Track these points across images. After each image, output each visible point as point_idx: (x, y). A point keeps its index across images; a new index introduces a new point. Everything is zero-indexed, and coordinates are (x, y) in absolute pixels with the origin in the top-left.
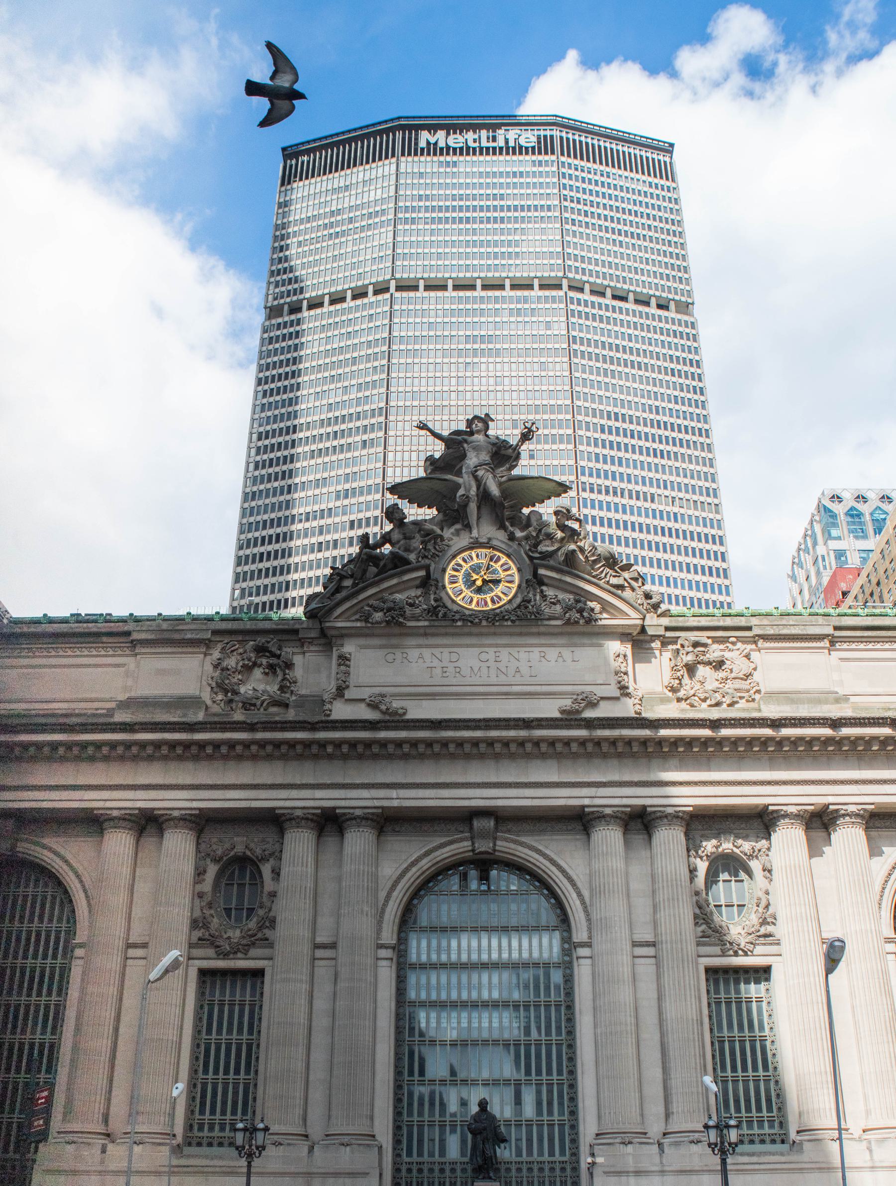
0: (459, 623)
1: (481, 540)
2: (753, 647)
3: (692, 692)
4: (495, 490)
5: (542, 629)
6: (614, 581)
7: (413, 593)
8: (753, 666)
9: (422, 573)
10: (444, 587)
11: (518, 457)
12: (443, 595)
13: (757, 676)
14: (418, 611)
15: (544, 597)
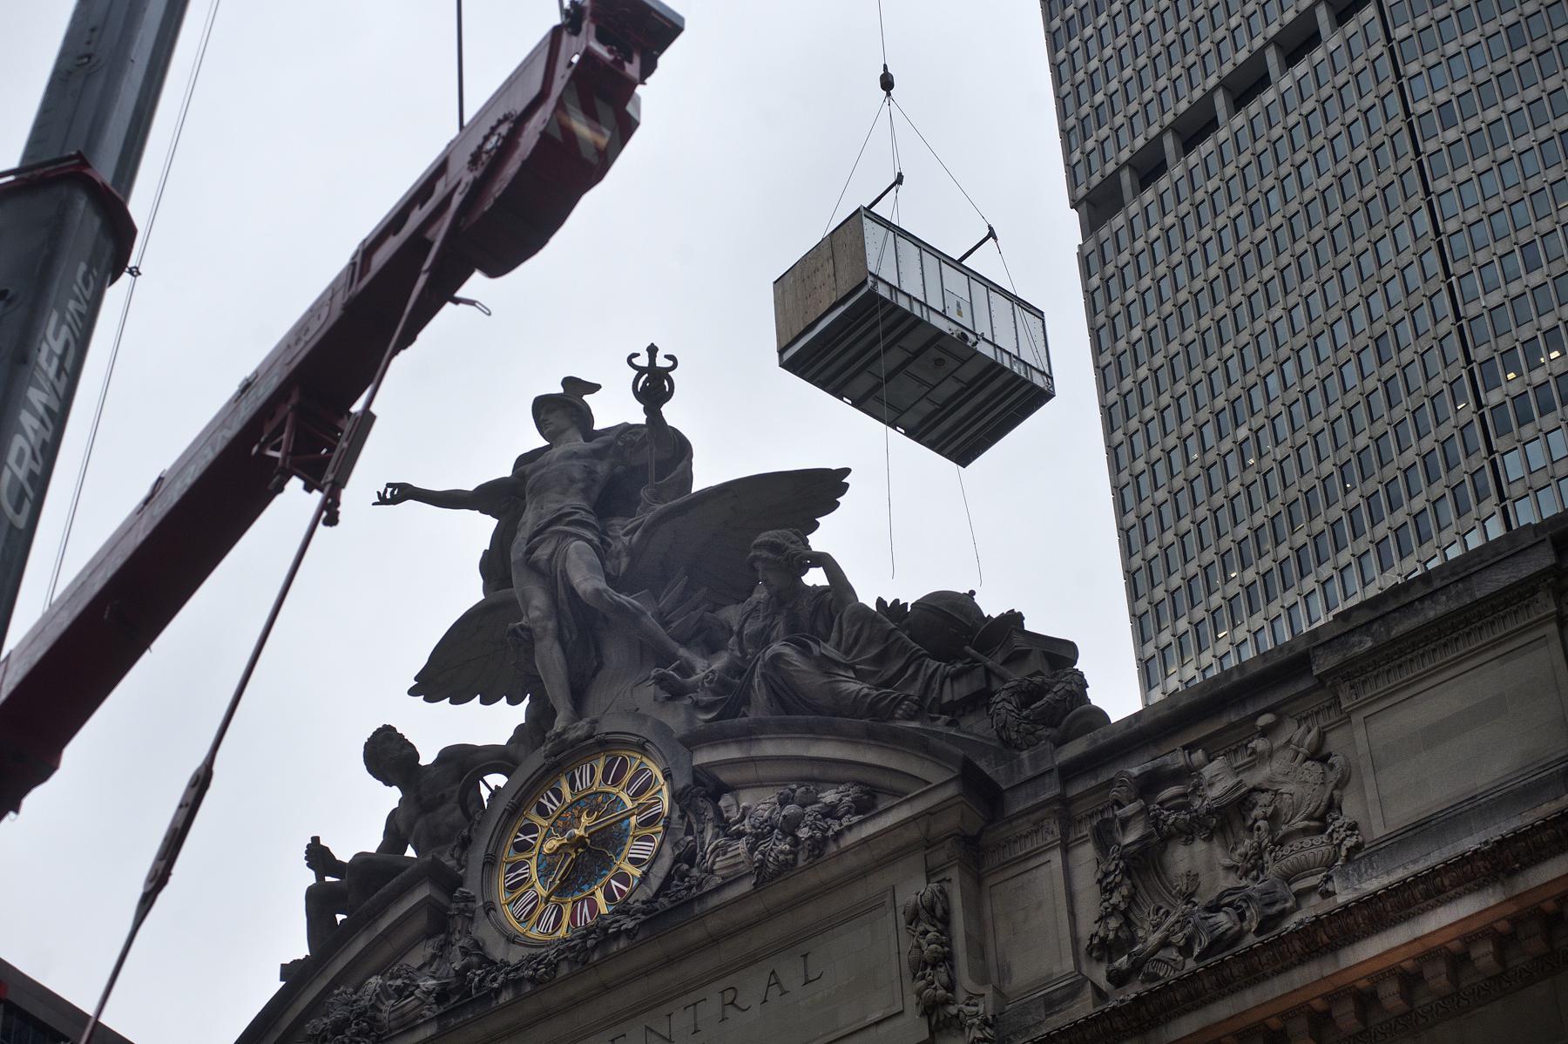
0: (506, 997)
1: (572, 735)
2: (1334, 717)
3: (1154, 938)
4: (585, 579)
5: (713, 924)
6: (962, 689)
7: (415, 959)
8: (1333, 777)
9: (422, 893)
10: (490, 907)
11: (679, 448)
12: (484, 931)
13: (1351, 809)
14: (410, 1003)
15: (723, 824)
